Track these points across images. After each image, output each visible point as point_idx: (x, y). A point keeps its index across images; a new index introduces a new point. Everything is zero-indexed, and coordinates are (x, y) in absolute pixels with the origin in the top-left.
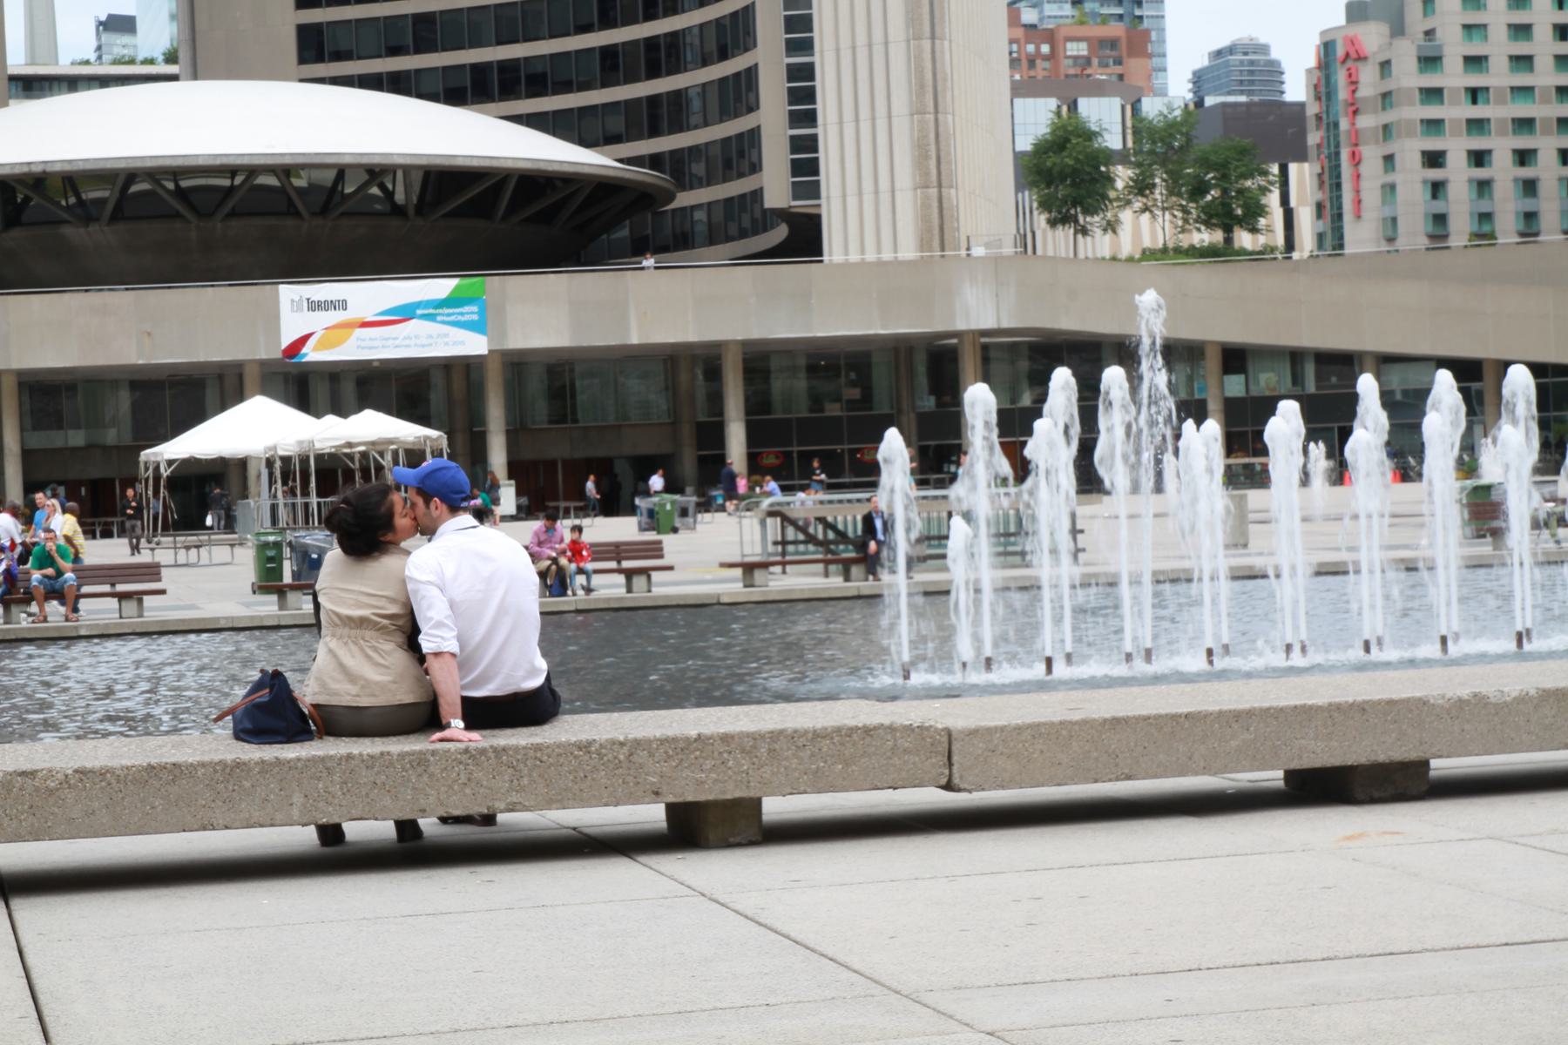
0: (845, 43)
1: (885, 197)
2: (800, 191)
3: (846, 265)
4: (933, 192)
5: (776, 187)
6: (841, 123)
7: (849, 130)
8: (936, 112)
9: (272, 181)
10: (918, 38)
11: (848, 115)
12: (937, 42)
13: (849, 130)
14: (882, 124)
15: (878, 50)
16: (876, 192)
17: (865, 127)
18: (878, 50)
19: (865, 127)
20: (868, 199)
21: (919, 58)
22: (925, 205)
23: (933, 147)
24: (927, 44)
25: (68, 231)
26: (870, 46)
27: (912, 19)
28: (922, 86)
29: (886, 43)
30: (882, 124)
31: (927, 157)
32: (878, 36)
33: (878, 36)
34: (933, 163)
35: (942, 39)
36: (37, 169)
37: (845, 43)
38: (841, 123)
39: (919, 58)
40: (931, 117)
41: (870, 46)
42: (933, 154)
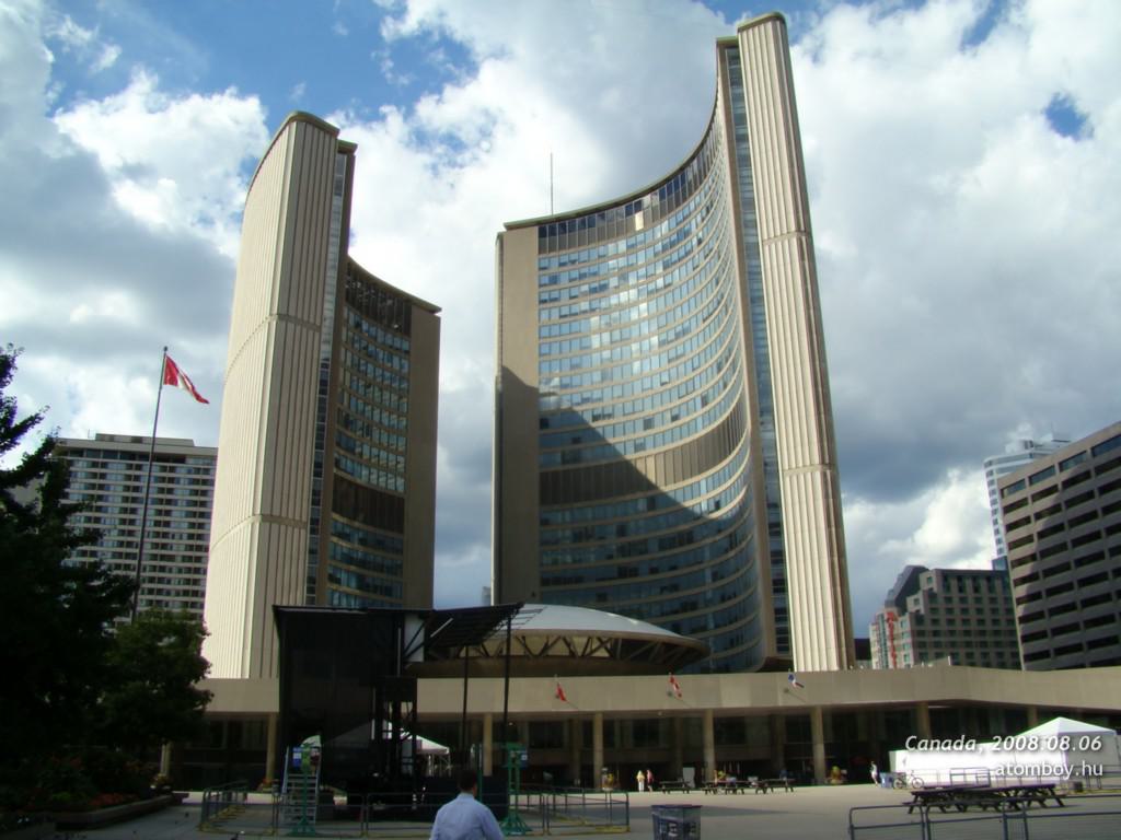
2: (780, 649)
5: (767, 648)
25: (483, 662)
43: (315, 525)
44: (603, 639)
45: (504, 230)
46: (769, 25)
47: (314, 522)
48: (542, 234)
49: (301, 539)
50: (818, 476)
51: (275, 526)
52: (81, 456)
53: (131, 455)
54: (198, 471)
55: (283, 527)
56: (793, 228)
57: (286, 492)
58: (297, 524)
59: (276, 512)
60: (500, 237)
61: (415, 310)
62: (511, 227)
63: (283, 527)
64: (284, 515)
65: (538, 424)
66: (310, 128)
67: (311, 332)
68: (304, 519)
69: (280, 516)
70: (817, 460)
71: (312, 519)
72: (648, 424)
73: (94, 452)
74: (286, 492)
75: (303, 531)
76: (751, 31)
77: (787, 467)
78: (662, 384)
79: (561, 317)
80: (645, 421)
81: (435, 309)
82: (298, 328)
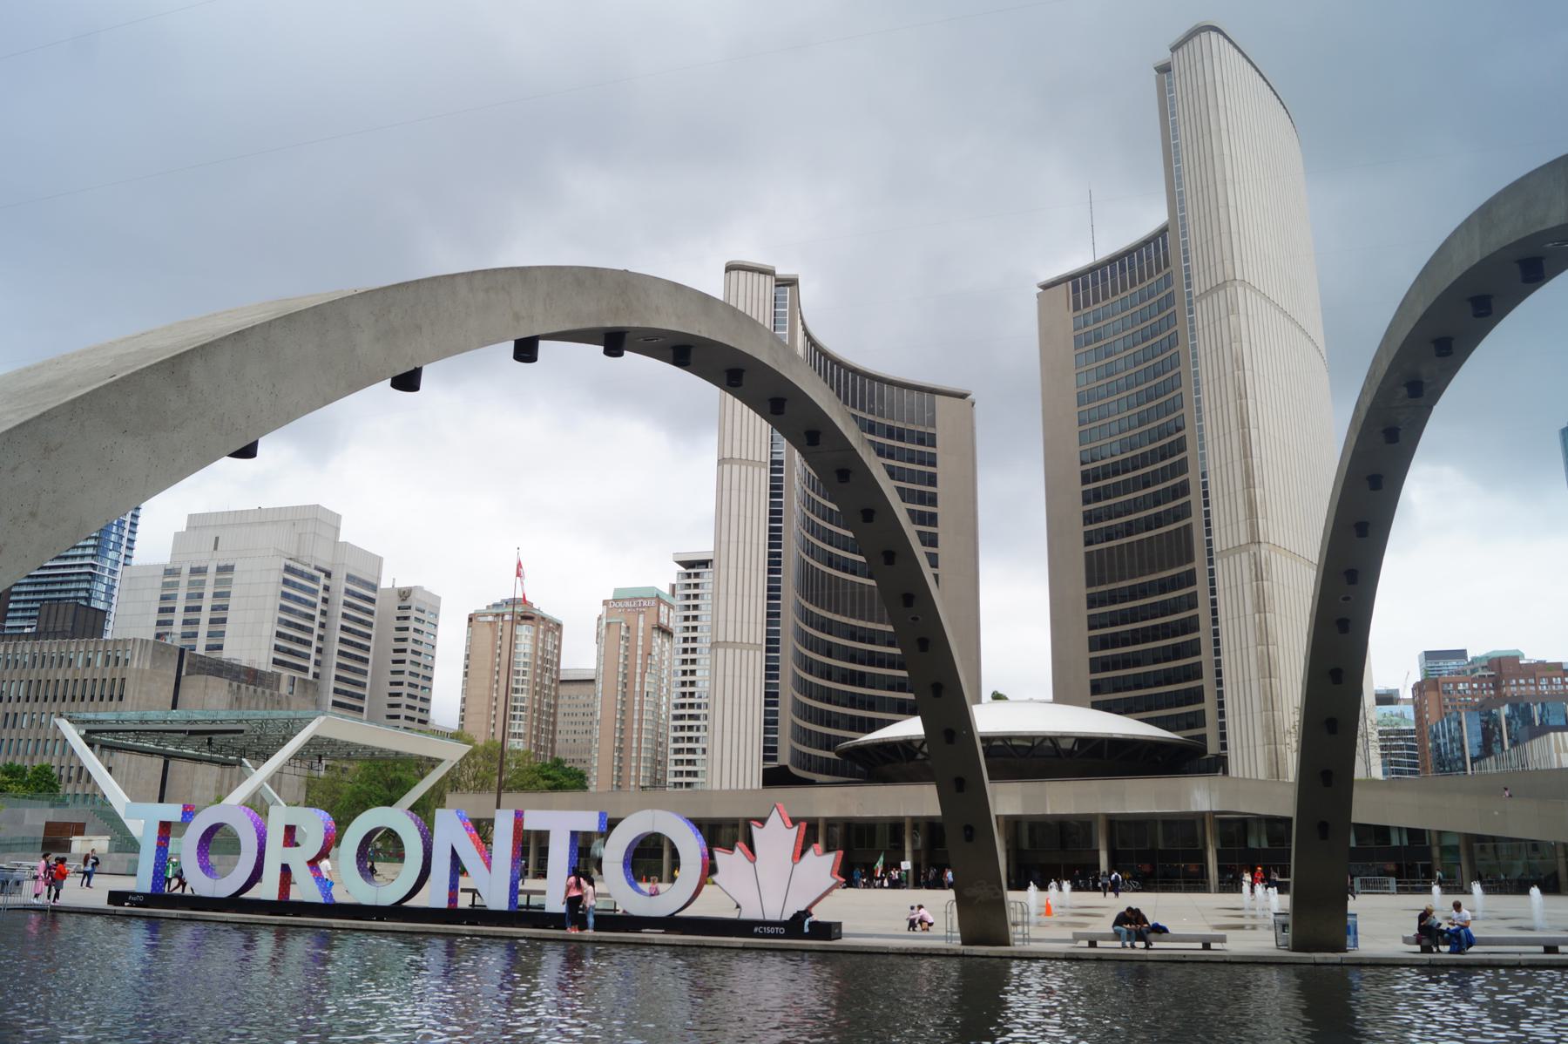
0: (1234, 680)
1: (1252, 750)
3: (1237, 778)
4: (1273, 746)
6: (1234, 716)
7: (1237, 718)
8: (1273, 710)
9: (1000, 743)
10: (1264, 677)
11: (1237, 712)
12: (1273, 679)
13: (1237, 718)
14: (1249, 716)
15: (1247, 683)
16: (1249, 747)
17: (1243, 717)
18: (1247, 683)
19: (1243, 717)
20: (1245, 750)
21: (1264, 686)
22: (1269, 753)
23: (1272, 726)
24: (1267, 680)
26: (1244, 681)
27: (1260, 668)
28: (1266, 698)
29: (1250, 680)
30: (1249, 716)
31: (1269, 731)
32: (1247, 677)
33: (1247, 677)
34: (1272, 733)
35: (1276, 678)
36: (909, 738)
37: (1234, 680)
38: (1234, 716)
39: (1264, 686)
40: (1271, 713)
41: (1244, 681)
42: (1272, 729)
43: (772, 644)
44: (1054, 740)
45: (1041, 290)
46: (1196, 40)
47: (768, 641)
48: (1075, 290)
50: (1245, 556)
51: (730, 652)
52: (707, 567)
55: (738, 651)
57: (739, 619)
59: (730, 639)
60: (1038, 295)
62: (1046, 287)
63: (738, 651)
64: (738, 640)
66: (742, 273)
67: (757, 470)
68: (759, 642)
69: (735, 642)
71: (767, 639)
74: (739, 619)
75: (758, 653)
76: (1180, 52)
81: (963, 396)
82: (743, 468)
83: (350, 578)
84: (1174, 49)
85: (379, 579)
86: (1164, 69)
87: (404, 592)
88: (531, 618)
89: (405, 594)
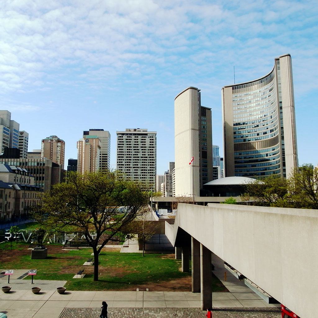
25: (229, 189)
48: (233, 89)
49: (198, 168)
53: (135, 134)
54: (150, 137)
56: (290, 105)
58: (197, 166)
61: (207, 110)
65: (233, 133)
70: (292, 153)
72: (258, 135)
73: (127, 134)
77: (286, 154)
78: (261, 117)
79: (238, 109)
80: (257, 134)
81: (210, 109)
83: (15, 130)
84: (280, 57)
85: (19, 129)
86: (277, 60)
87: (21, 133)
88: (60, 141)
89: (22, 133)
